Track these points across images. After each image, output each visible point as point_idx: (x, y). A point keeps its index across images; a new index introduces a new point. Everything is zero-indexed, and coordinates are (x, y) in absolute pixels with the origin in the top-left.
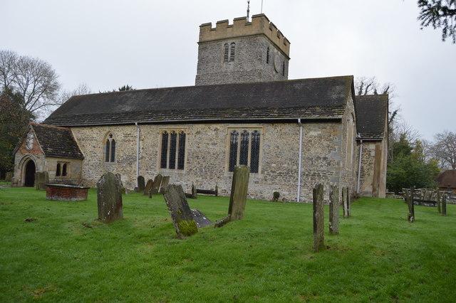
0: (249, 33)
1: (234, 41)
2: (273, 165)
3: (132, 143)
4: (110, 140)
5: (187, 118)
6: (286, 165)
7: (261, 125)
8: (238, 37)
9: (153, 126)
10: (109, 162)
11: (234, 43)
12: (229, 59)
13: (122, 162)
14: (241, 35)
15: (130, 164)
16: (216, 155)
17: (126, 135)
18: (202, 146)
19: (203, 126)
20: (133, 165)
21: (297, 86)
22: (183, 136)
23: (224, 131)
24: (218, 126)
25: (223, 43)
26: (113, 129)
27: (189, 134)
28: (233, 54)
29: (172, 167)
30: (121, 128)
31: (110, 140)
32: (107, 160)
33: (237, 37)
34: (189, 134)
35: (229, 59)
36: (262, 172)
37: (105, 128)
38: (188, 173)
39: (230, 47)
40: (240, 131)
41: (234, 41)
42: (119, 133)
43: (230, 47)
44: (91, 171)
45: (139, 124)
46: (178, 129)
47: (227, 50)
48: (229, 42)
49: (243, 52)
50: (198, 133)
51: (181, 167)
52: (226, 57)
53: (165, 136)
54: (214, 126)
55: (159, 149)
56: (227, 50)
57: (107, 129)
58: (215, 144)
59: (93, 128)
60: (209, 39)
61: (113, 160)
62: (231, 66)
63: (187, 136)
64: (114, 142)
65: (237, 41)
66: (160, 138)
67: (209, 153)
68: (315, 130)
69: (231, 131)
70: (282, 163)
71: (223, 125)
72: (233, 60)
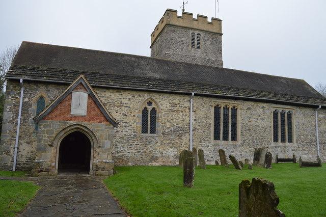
0: (211, 30)
1: (199, 32)
2: (302, 137)
3: (181, 114)
4: (150, 108)
5: (241, 95)
6: (309, 137)
7: (295, 108)
8: (203, 30)
9: (205, 99)
10: (149, 134)
11: (199, 34)
12: (196, 46)
13: (168, 134)
14: (205, 29)
15: (180, 136)
16: (265, 129)
17: (174, 105)
18: (253, 122)
19: (252, 103)
20: (184, 138)
21: (282, 81)
22: (234, 110)
23: (269, 109)
24: (265, 105)
25: (191, 32)
26: (154, 96)
27: (241, 109)
28: (198, 43)
29: (226, 138)
30: (166, 96)
31: (150, 108)
32: (144, 130)
33: (203, 31)
34: (241, 109)
35: (196, 46)
36: (296, 142)
37: (142, 94)
38: (242, 144)
39: (196, 37)
40: (280, 110)
41: (199, 32)
42: (163, 103)
43: (196, 37)
44: (120, 146)
45: (196, 95)
46: (231, 104)
47: (193, 38)
48: (196, 33)
49: (208, 43)
50: (249, 109)
51: (234, 138)
52: (193, 45)
53: (217, 109)
54: (261, 105)
55: (212, 121)
56: (193, 38)
57: (146, 96)
58: (263, 119)
59: (122, 92)
60: (177, 24)
61: (153, 131)
62: (198, 53)
63: (239, 112)
64: (154, 110)
65: (202, 34)
66: (213, 110)
67: (259, 127)
68: (322, 114)
69: (273, 110)
70: (307, 136)
71: (268, 104)
72: (198, 48)
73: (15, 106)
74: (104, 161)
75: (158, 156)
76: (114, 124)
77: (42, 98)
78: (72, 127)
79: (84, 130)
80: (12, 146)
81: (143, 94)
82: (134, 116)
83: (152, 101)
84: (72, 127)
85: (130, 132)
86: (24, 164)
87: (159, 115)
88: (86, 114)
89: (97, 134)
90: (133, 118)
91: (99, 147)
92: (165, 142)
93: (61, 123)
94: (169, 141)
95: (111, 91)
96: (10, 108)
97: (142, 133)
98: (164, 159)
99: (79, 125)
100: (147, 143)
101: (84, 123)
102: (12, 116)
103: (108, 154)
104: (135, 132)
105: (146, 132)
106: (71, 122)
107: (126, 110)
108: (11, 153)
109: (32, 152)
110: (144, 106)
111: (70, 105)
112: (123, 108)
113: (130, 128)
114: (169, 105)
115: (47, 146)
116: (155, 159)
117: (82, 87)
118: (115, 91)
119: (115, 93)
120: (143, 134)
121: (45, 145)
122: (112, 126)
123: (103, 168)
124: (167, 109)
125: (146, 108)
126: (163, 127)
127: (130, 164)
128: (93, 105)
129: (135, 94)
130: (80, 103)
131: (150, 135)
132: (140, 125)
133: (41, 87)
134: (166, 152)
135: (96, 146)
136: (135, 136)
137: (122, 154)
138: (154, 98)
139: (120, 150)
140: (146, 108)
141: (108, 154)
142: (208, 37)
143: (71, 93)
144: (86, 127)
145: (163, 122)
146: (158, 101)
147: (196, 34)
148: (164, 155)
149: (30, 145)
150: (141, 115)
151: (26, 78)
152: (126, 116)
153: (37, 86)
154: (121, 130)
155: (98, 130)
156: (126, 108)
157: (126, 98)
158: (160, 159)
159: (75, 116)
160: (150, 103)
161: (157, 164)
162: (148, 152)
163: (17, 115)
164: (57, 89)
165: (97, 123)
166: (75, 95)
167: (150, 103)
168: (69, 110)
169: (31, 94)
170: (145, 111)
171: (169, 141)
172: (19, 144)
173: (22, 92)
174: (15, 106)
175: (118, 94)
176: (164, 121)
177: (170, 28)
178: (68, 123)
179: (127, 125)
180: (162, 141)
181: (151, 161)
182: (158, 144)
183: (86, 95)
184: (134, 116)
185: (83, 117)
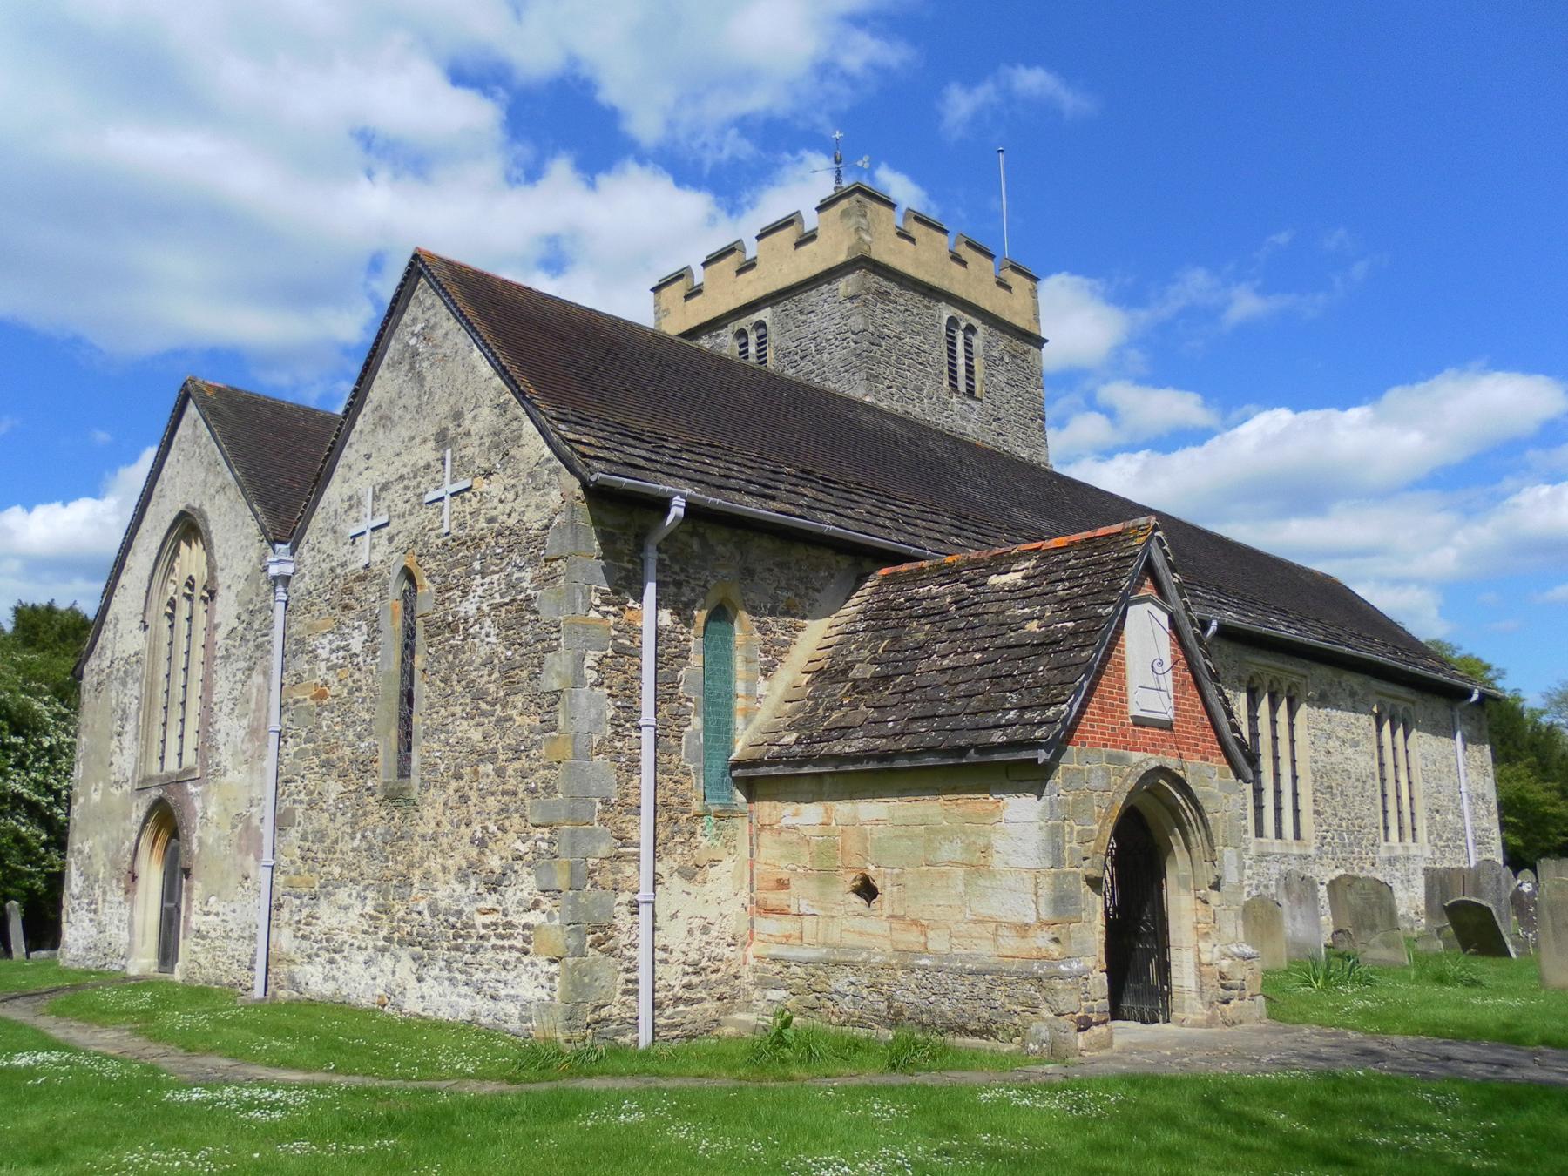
1: (975, 322)
12: (962, 387)
25: (946, 311)
73: (620, 651)
80: (625, 897)
86: (677, 1000)
96: (600, 663)
109: (705, 930)
133: (720, 549)
142: (1003, 342)
147: (963, 325)
163: (630, 710)
164: (781, 565)
173: (651, 568)
174: (620, 651)
177: (874, 281)
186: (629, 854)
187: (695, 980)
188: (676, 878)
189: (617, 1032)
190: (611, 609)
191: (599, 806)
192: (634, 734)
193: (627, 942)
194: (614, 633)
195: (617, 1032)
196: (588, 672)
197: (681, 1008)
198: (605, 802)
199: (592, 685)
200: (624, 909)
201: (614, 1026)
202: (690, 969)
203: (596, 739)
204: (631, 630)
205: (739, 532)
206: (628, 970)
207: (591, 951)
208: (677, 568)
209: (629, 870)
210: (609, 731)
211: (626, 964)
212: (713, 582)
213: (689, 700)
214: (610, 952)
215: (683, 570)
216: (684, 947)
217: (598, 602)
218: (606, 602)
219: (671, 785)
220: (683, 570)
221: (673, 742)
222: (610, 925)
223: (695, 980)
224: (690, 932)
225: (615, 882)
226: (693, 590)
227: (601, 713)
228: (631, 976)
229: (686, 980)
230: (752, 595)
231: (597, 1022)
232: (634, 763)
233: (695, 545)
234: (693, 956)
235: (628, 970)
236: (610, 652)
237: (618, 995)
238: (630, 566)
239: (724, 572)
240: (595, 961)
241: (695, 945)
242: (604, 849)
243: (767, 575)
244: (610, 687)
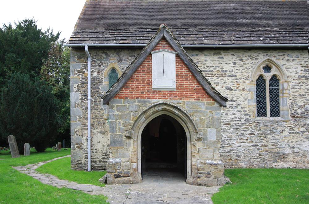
4: (268, 76)
26: (275, 57)
31: (268, 76)
32: (261, 112)
37: (254, 54)
57: (262, 58)
59: (220, 53)
61: (275, 112)
64: (275, 79)
73: (83, 83)
74: (209, 162)
75: (286, 151)
76: (221, 101)
77: (113, 70)
78: (156, 109)
79: (174, 113)
80: (85, 138)
81: (256, 55)
82: (244, 90)
83: (270, 65)
84: (156, 109)
85: (239, 114)
86: (100, 161)
87: (283, 85)
88: (174, 87)
89: (195, 119)
90: (242, 92)
91: (199, 139)
92: (296, 130)
93: (139, 102)
94: (303, 129)
95: (206, 52)
96: (78, 86)
97: (258, 115)
98: (298, 158)
99: (166, 104)
100: (268, 132)
101: (173, 101)
102: (80, 98)
103: (214, 151)
104: (246, 115)
105: (265, 115)
106: (154, 101)
107: (230, 81)
108: (85, 147)
110: (259, 73)
111: (150, 74)
112: (226, 79)
113: (239, 108)
114: (300, 68)
115: (124, 139)
116: (282, 157)
117: (165, 44)
118: (213, 52)
119: (212, 56)
120: (259, 118)
121: (121, 136)
122: (216, 105)
123: (209, 174)
124: (297, 76)
125: (261, 76)
126: (292, 105)
127: (243, 165)
128: (185, 71)
129: (242, 55)
130: (164, 68)
131: (272, 118)
132: (254, 104)
133: (111, 55)
134: (298, 146)
135: (194, 136)
136: (247, 120)
137: (230, 148)
138: (274, 59)
139: (226, 142)
140: (261, 76)
141: (214, 151)
143: (150, 55)
144: (179, 110)
145: (291, 98)
146: (280, 63)
148: (296, 150)
149: (104, 136)
150: (254, 87)
151: (92, 44)
152: (232, 90)
153: (107, 54)
154: (226, 112)
155: (196, 112)
156: (230, 78)
157: (228, 63)
158: (291, 157)
159: (159, 91)
160: (267, 69)
161: (285, 166)
162: (270, 146)
163: (86, 96)
165: (192, 100)
166: (157, 57)
167: (267, 69)
168: (150, 82)
169: (100, 66)
170: (260, 81)
171: (303, 129)
172: (93, 134)
174: (83, 83)
175: (216, 57)
176: (293, 94)
178: (149, 102)
179: (234, 104)
180: (292, 129)
181: (275, 161)
182: (286, 133)
183: (171, 57)
184: (244, 90)
185: (171, 91)
186: (86, 128)
187: (106, 157)
188: (99, 134)
189: (84, 167)
190: (80, 74)
191: (78, 118)
192: (87, 101)
193: (86, 147)
194: (81, 79)
195: (84, 167)
196: (74, 89)
197: (102, 163)
198: (80, 117)
199: (75, 91)
200: (85, 140)
201: (83, 165)
202: (104, 155)
203: (77, 103)
204: (86, 78)
205: (117, 50)
206: (86, 153)
207: (76, 149)
208: (99, 62)
209: (86, 132)
210: (80, 101)
211: (86, 152)
212: (109, 64)
213: (103, 93)
214: (82, 149)
215: (100, 62)
216: (102, 149)
217: (77, 73)
218: (79, 72)
219: (97, 112)
220: (100, 62)
221: (98, 103)
222: (81, 143)
223: (106, 157)
224: (104, 146)
225: (82, 134)
226: (104, 66)
227: (78, 97)
228: (86, 155)
229: (103, 157)
230: (122, 65)
231: (78, 164)
232: (87, 108)
233: (104, 56)
234: (105, 151)
235: (86, 153)
236: (80, 84)
237: (84, 159)
238: (85, 63)
239: (113, 61)
240: (77, 151)
241: (105, 149)
242: (79, 127)
243: (127, 59)
244: (80, 91)
